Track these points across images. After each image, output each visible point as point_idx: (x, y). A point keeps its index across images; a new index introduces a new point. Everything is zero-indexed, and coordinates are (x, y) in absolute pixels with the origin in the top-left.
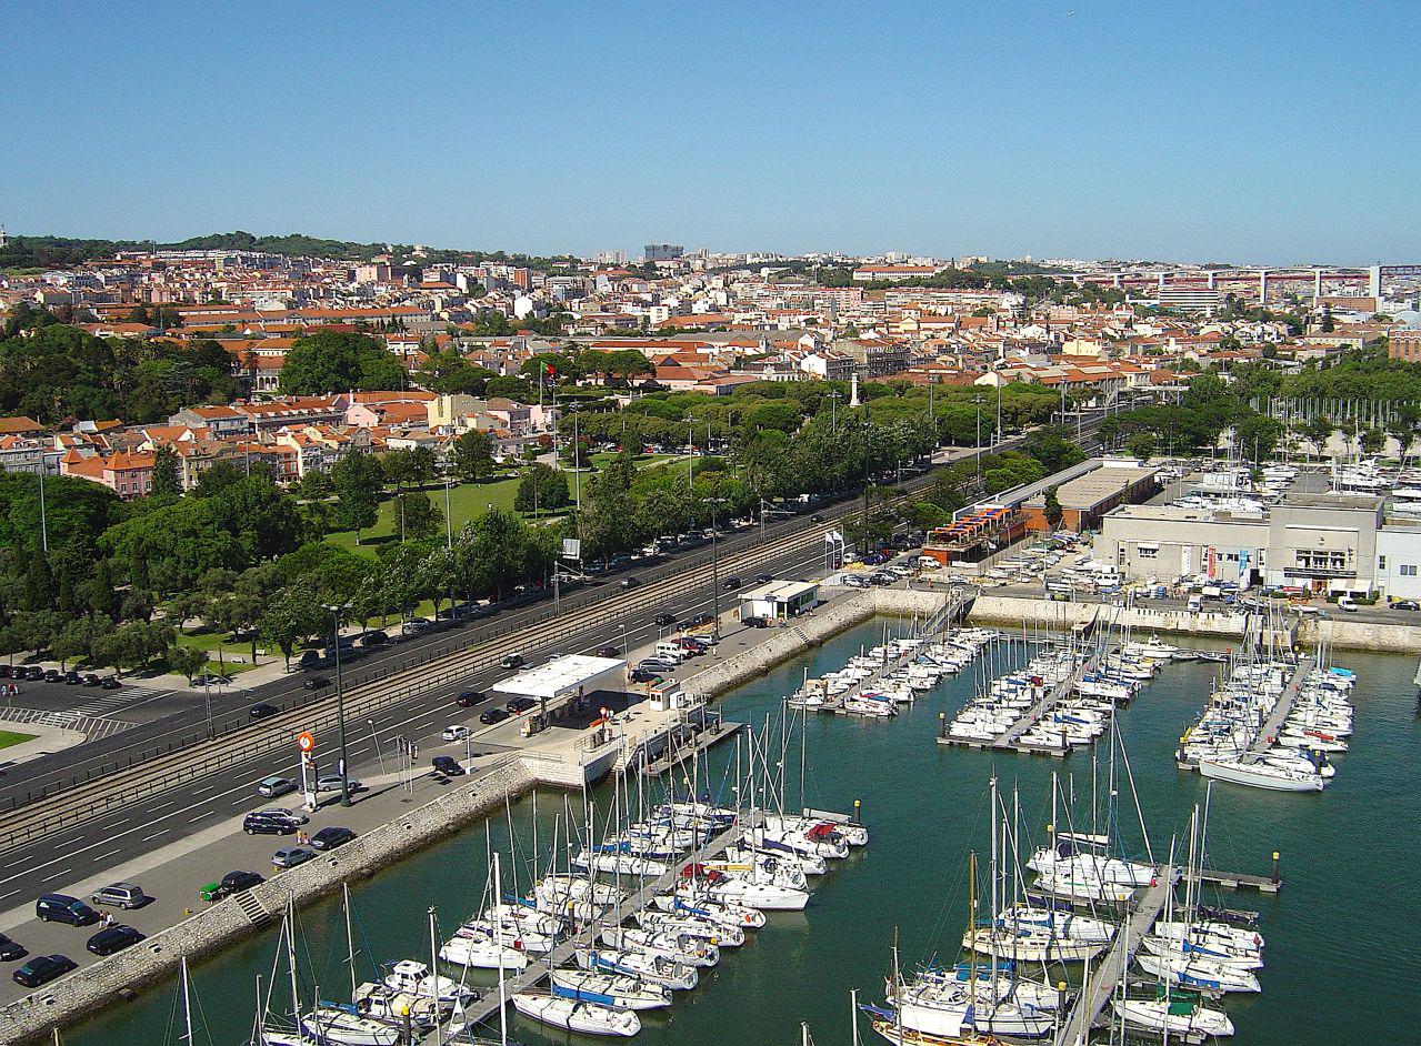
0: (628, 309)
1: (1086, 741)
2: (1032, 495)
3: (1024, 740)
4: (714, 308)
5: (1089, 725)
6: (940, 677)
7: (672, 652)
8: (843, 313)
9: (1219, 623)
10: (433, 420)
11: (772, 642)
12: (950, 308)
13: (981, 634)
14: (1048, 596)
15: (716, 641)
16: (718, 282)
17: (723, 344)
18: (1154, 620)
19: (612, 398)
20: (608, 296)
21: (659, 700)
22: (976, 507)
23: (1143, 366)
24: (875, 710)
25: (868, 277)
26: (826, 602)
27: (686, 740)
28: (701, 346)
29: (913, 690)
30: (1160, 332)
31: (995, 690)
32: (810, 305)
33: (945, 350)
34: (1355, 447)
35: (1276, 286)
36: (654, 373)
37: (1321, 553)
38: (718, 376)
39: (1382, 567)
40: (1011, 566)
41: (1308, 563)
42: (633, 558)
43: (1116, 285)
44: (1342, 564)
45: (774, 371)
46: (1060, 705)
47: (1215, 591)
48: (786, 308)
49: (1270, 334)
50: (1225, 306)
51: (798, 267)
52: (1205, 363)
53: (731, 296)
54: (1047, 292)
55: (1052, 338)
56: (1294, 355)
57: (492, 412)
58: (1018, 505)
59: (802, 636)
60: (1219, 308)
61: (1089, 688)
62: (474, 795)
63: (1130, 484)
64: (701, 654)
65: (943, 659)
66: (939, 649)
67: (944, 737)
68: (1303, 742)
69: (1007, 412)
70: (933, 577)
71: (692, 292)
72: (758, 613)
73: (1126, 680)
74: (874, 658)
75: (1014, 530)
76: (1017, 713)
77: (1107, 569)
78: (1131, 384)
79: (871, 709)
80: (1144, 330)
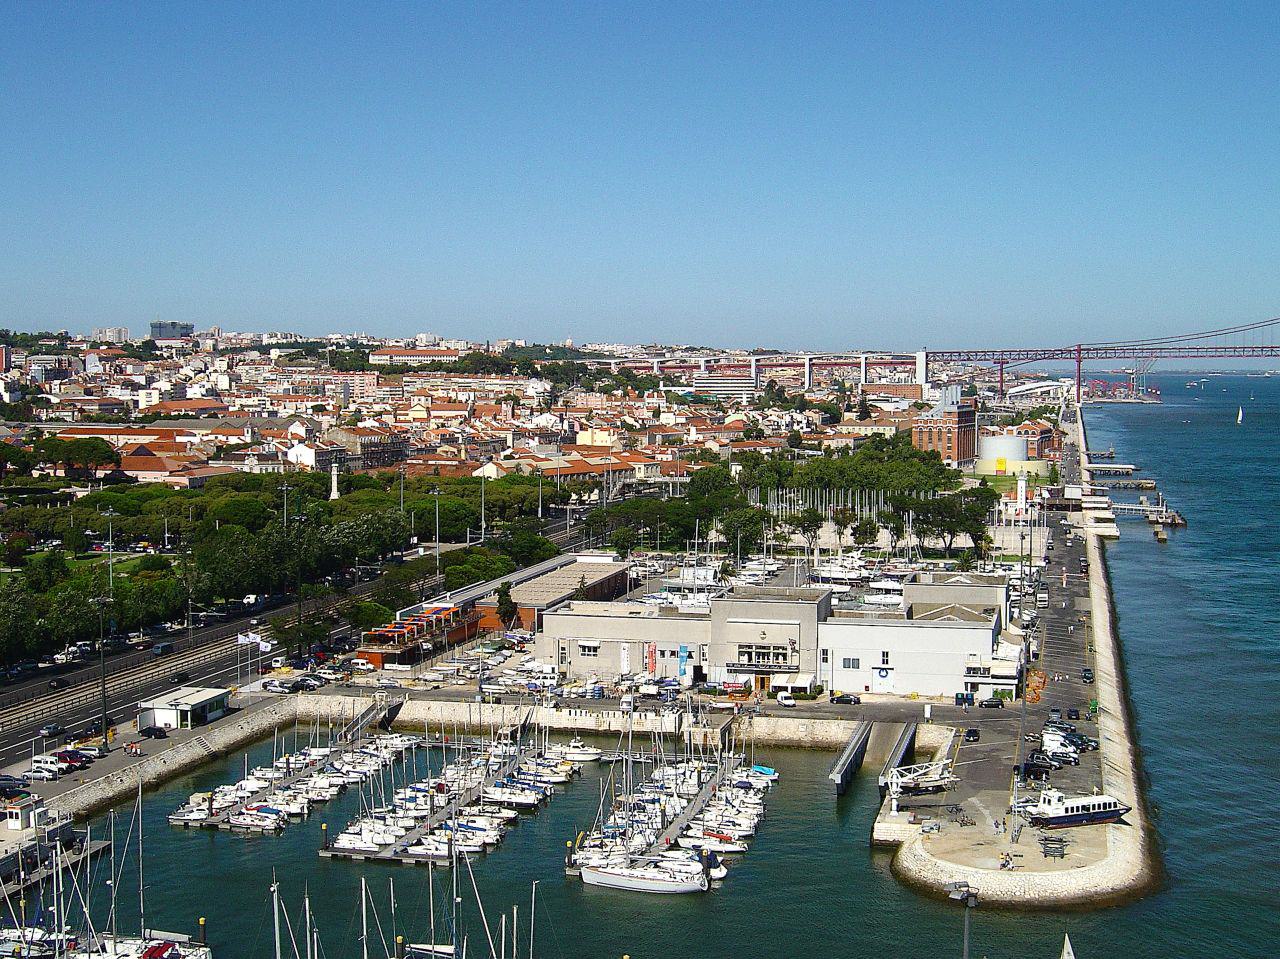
0: (117, 393)
1: (477, 849)
2: (486, 593)
3: (412, 850)
4: (213, 392)
5: (486, 830)
6: (343, 787)
7: (48, 766)
8: (355, 399)
9: (650, 722)
11: (167, 754)
12: (472, 394)
13: (398, 742)
14: (478, 698)
15: (104, 751)
16: (221, 364)
17: (204, 432)
18: (586, 721)
19: (68, 490)
20: (94, 378)
21: (17, 818)
22: (424, 606)
23: (659, 457)
24: (260, 823)
25: (383, 360)
26: (239, 709)
27: (43, 862)
28: (181, 433)
29: (310, 801)
30: (683, 420)
31: (396, 800)
32: (319, 390)
33: (450, 440)
34: (848, 539)
35: (825, 372)
36: (118, 463)
37: (764, 648)
38: (192, 466)
39: (825, 660)
40: (449, 668)
41: (750, 659)
42: (40, 665)
43: (656, 371)
44: (785, 659)
45: (256, 462)
46: (461, 813)
47: (653, 690)
48: (296, 393)
49: (799, 423)
50: (763, 393)
51: (311, 349)
52: (725, 454)
53: (234, 379)
54: (578, 379)
55: (566, 427)
56: (820, 444)
58: (472, 603)
59: (205, 746)
60: (756, 396)
61: (497, 794)
63: (589, 582)
64: (83, 767)
65: (350, 768)
66: (348, 757)
67: (327, 849)
68: (697, 843)
69: (494, 506)
70: (359, 680)
71: (192, 374)
72: (160, 724)
73: (539, 784)
74: (278, 769)
75: (464, 628)
76: (411, 823)
77: (547, 669)
78: (640, 475)
79: (257, 822)
80: (667, 419)
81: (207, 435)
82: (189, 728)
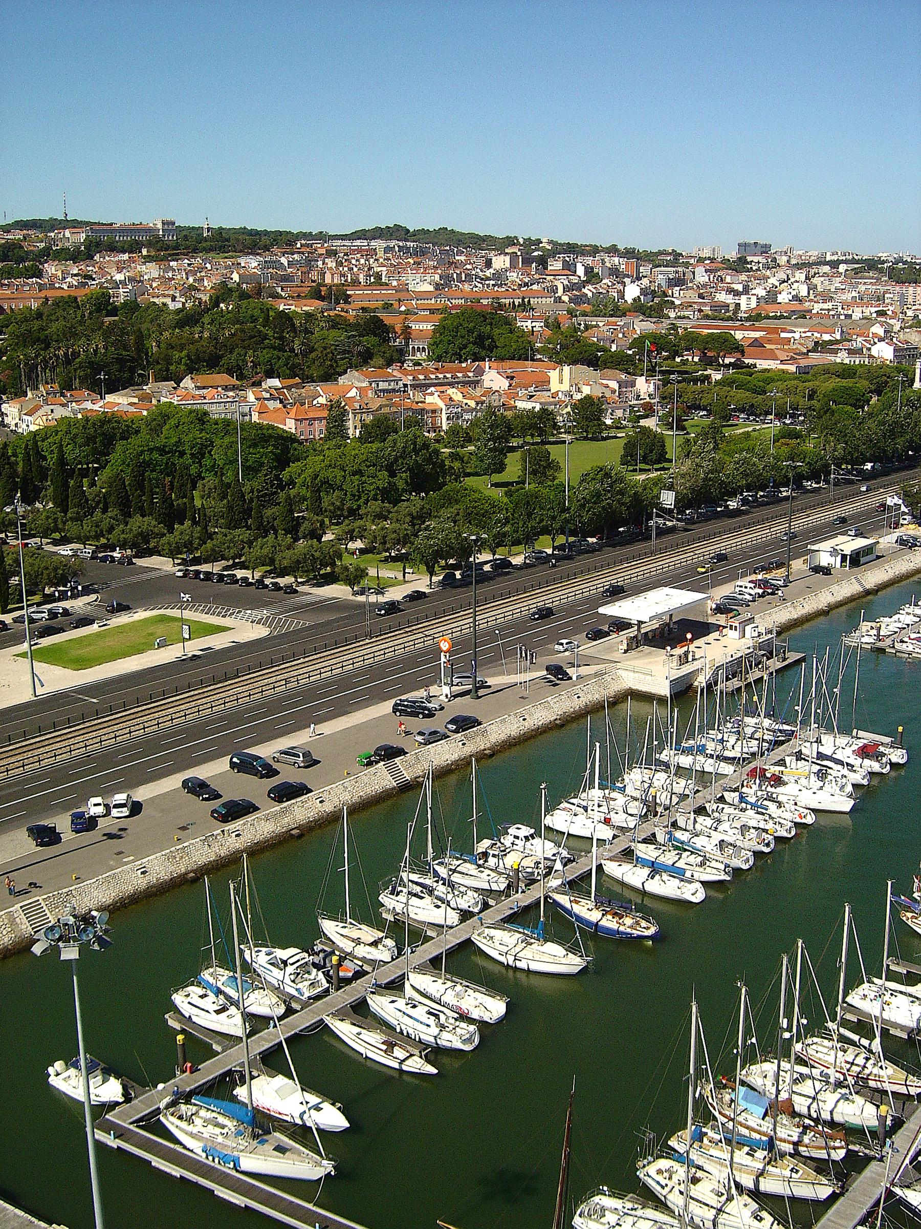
0: (723, 297)
4: (796, 298)
7: (748, 590)
8: (910, 306)
10: (554, 386)
11: (835, 588)
15: (787, 582)
19: (705, 373)
20: (705, 286)
21: (736, 630)
26: (883, 556)
27: (757, 665)
28: (784, 330)
32: (880, 298)
36: (743, 353)
38: (798, 357)
42: (719, 509)
45: (847, 355)
48: (860, 300)
51: (872, 265)
53: (812, 288)
57: (605, 382)
59: (861, 584)
62: (578, 697)
64: (773, 594)
71: (777, 284)
72: (824, 563)
81: (805, 332)
82: (848, 568)
